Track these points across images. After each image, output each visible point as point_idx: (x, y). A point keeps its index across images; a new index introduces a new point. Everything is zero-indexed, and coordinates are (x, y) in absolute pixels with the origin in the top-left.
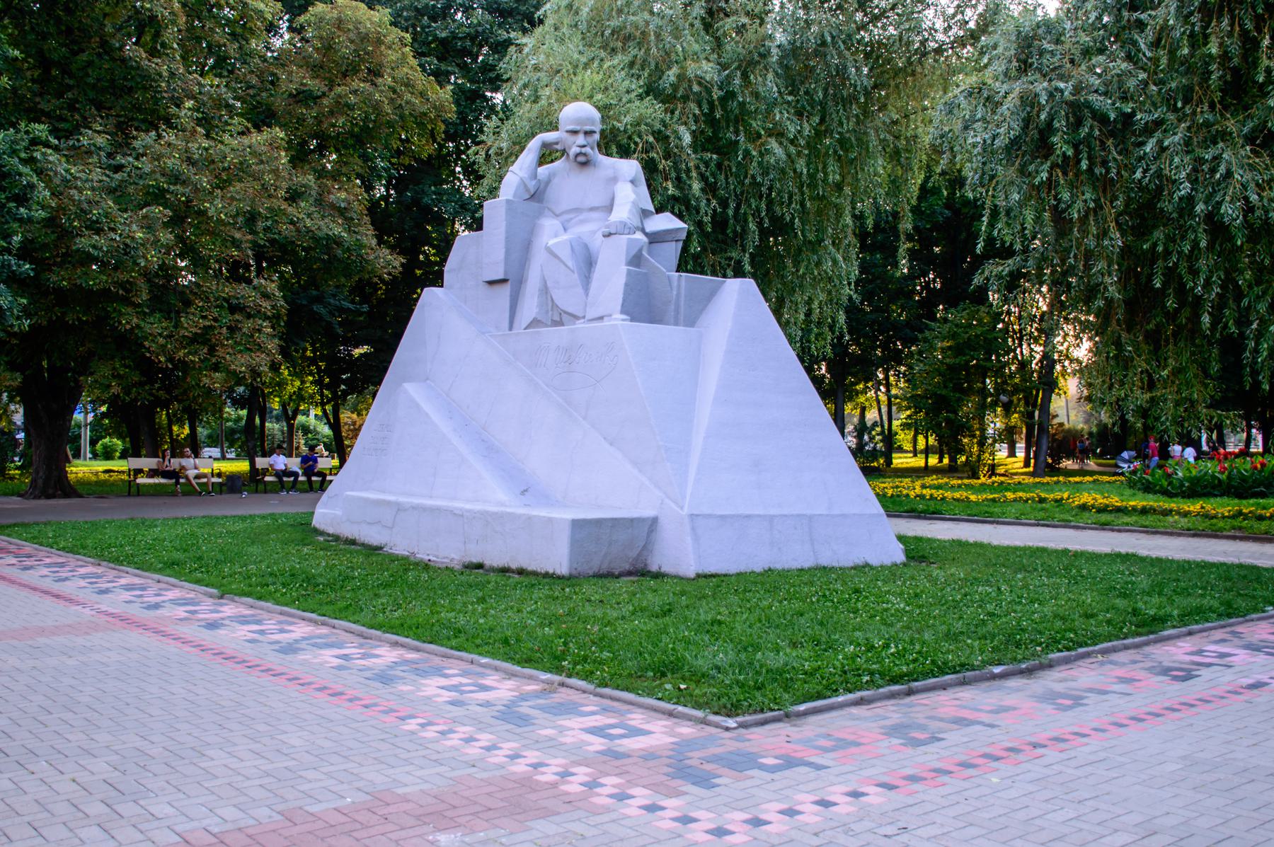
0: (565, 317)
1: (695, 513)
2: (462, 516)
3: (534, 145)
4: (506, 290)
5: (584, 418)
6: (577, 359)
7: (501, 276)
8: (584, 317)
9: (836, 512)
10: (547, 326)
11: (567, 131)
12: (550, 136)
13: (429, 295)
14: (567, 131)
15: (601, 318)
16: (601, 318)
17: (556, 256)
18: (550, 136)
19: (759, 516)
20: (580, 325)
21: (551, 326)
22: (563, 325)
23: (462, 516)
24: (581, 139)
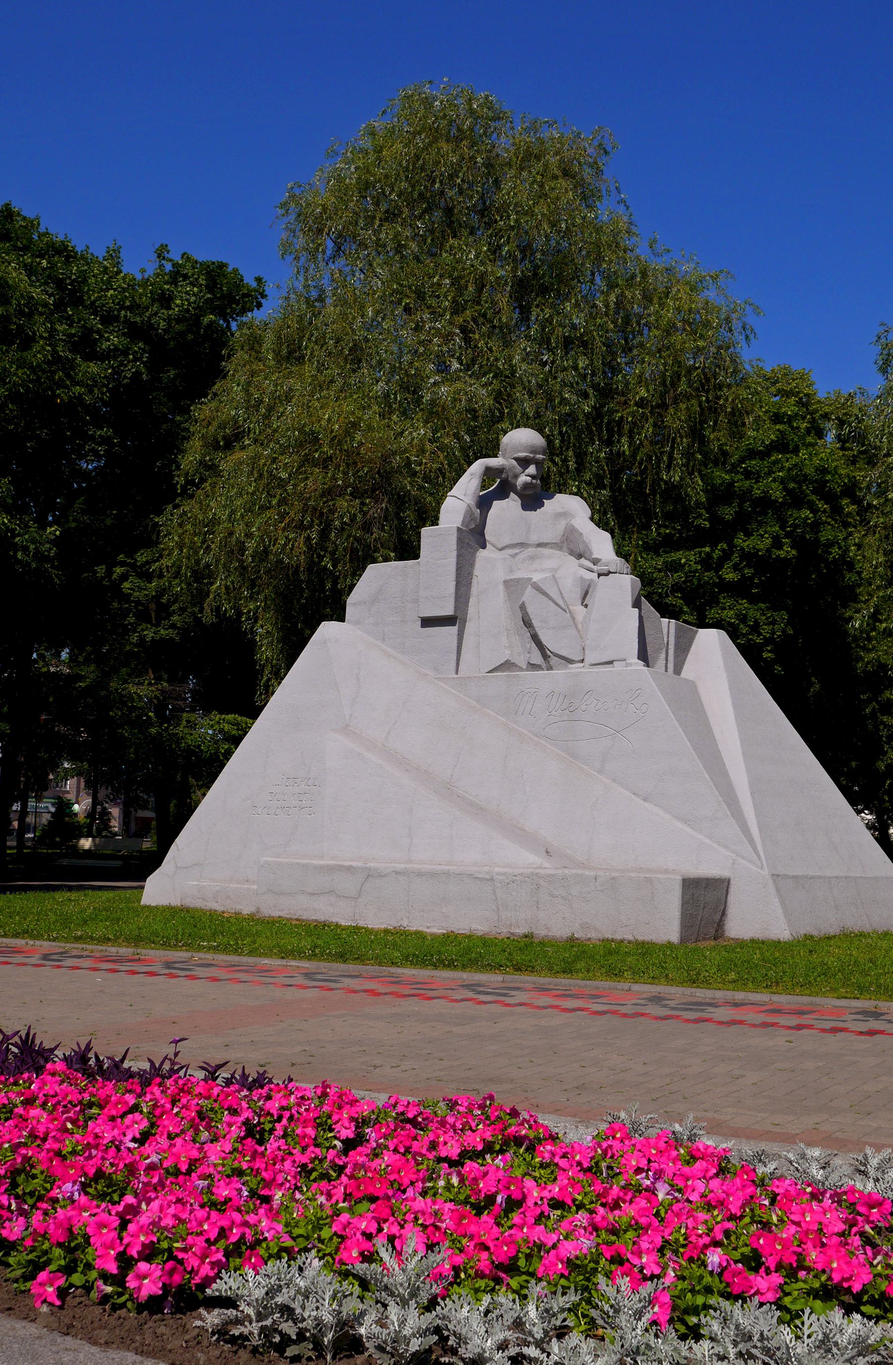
0: (554, 660)
1: (776, 873)
2: (492, 880)
3: (478, 466)
4: (453, 630)
5: (600, 772)
6: (583, 707)
7: (448, 610)
8: (582, 661)
9: (869, 875)
10: (521, 669)
11: (516, 459)
12: (493, 462)
13: (327, 629)
14: (516, 459)
15: (611, 662)
16: (611, 662)
17: (545, 594)
18: (493, 462)
19: (820, 877)
20: (575, 668)
21: (527, 670)
22: (550, 668)
23: (492, 880)
24: (532, 470)
